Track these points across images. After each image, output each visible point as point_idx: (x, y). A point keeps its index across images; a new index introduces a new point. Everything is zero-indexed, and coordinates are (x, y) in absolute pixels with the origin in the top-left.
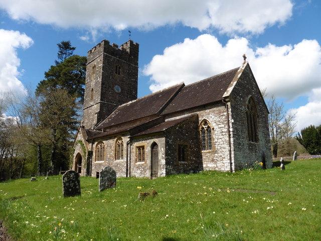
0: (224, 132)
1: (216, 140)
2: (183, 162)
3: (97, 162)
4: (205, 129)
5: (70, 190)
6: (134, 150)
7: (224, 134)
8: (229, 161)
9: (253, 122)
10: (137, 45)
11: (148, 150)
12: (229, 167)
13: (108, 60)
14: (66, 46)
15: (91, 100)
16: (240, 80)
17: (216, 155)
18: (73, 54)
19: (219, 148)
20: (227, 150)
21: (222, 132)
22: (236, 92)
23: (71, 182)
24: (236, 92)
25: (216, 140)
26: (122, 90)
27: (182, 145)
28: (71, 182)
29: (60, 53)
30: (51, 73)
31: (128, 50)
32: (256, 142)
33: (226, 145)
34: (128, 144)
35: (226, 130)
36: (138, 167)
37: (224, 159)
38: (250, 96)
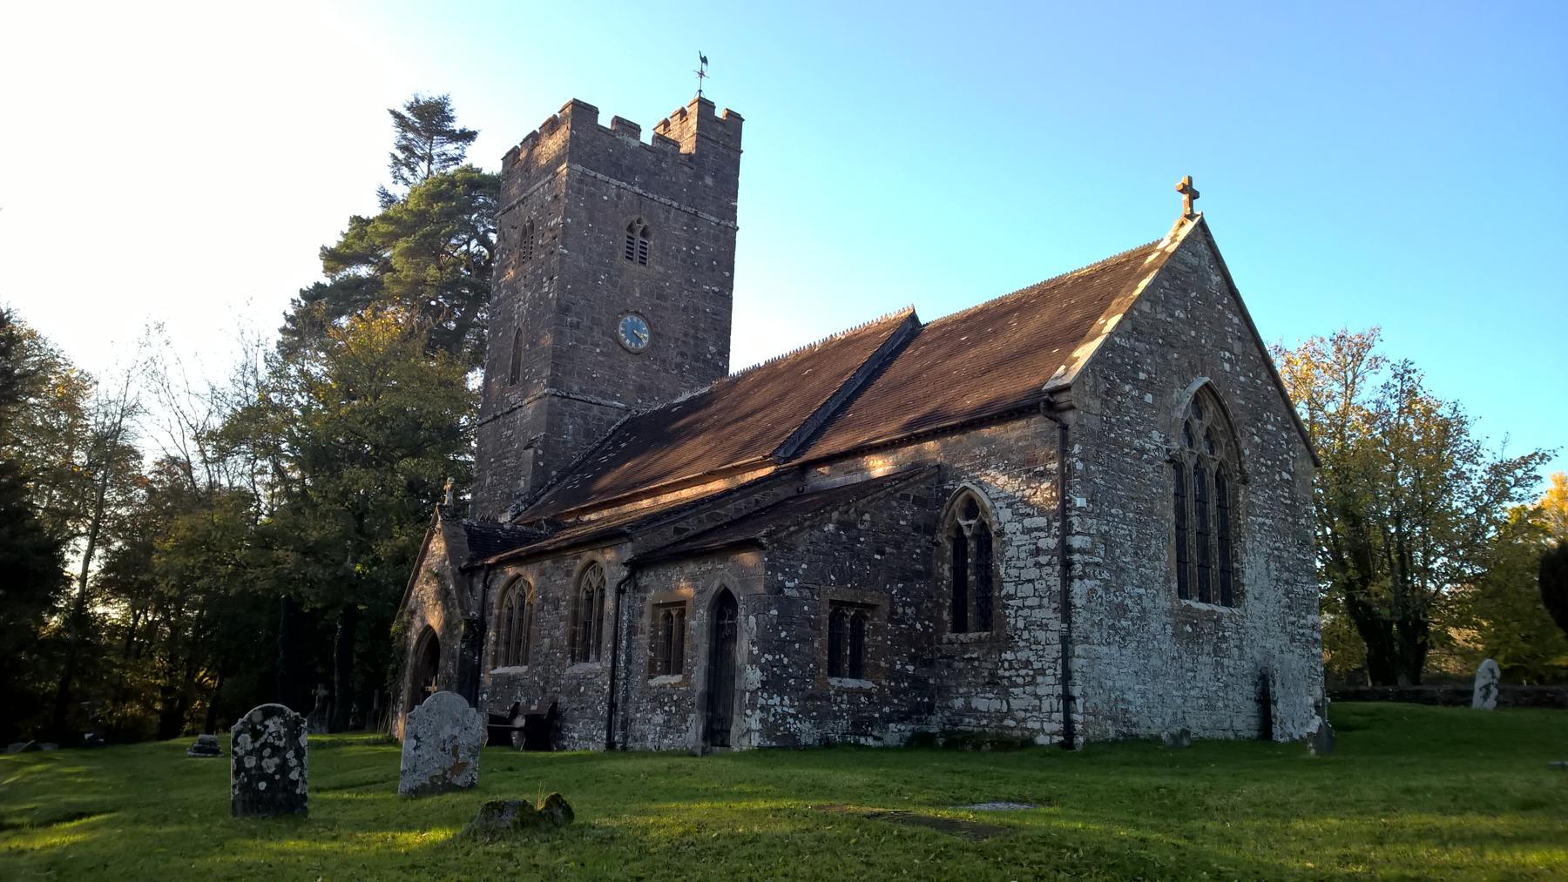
0: (1046, 552)
1: (1009, 588)
2: (851, 683)
3: (500, 670)
4: (967, 533)
5: (262, 785)
6: (645, 622)
7: (1043, 559)
8: (1059, 689)
9: (1212, 507)
10: (735, 120)
11: (698, 622)
12: (1059, 716)
13: (591, 195)
14: (429, 120)
15: (513, 382)
16: (1146, 307)
17: (1009, 655)
18: (464, 163)
19: (1021, 624)
20: (1056, 636)
21: (1038, 551)
22: (1113, 367)
23: (267, 752)
24: (1113, 367)
25: (1009, 588)
26: (655, 335)
27: (851, 605)
28: (267, 752)
29: (401, 156)
30: (358, 247)
31: (688, 146)
32: (1227, 603)
33: (1049, 614)
34: (620, 591)
35: (1052, 543)
36: (658, 699)
37: (1040, 679)
38: (1198, 383)
